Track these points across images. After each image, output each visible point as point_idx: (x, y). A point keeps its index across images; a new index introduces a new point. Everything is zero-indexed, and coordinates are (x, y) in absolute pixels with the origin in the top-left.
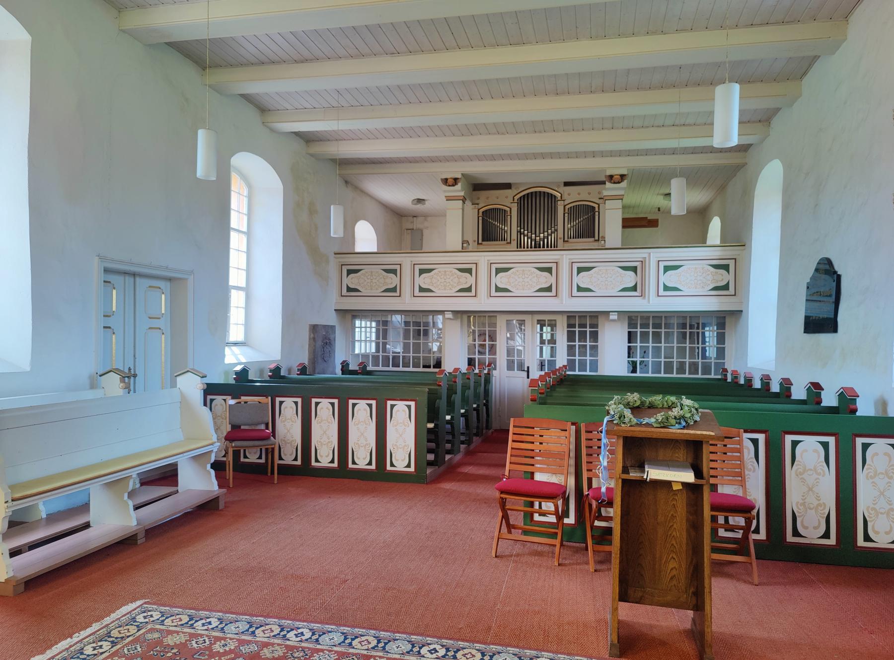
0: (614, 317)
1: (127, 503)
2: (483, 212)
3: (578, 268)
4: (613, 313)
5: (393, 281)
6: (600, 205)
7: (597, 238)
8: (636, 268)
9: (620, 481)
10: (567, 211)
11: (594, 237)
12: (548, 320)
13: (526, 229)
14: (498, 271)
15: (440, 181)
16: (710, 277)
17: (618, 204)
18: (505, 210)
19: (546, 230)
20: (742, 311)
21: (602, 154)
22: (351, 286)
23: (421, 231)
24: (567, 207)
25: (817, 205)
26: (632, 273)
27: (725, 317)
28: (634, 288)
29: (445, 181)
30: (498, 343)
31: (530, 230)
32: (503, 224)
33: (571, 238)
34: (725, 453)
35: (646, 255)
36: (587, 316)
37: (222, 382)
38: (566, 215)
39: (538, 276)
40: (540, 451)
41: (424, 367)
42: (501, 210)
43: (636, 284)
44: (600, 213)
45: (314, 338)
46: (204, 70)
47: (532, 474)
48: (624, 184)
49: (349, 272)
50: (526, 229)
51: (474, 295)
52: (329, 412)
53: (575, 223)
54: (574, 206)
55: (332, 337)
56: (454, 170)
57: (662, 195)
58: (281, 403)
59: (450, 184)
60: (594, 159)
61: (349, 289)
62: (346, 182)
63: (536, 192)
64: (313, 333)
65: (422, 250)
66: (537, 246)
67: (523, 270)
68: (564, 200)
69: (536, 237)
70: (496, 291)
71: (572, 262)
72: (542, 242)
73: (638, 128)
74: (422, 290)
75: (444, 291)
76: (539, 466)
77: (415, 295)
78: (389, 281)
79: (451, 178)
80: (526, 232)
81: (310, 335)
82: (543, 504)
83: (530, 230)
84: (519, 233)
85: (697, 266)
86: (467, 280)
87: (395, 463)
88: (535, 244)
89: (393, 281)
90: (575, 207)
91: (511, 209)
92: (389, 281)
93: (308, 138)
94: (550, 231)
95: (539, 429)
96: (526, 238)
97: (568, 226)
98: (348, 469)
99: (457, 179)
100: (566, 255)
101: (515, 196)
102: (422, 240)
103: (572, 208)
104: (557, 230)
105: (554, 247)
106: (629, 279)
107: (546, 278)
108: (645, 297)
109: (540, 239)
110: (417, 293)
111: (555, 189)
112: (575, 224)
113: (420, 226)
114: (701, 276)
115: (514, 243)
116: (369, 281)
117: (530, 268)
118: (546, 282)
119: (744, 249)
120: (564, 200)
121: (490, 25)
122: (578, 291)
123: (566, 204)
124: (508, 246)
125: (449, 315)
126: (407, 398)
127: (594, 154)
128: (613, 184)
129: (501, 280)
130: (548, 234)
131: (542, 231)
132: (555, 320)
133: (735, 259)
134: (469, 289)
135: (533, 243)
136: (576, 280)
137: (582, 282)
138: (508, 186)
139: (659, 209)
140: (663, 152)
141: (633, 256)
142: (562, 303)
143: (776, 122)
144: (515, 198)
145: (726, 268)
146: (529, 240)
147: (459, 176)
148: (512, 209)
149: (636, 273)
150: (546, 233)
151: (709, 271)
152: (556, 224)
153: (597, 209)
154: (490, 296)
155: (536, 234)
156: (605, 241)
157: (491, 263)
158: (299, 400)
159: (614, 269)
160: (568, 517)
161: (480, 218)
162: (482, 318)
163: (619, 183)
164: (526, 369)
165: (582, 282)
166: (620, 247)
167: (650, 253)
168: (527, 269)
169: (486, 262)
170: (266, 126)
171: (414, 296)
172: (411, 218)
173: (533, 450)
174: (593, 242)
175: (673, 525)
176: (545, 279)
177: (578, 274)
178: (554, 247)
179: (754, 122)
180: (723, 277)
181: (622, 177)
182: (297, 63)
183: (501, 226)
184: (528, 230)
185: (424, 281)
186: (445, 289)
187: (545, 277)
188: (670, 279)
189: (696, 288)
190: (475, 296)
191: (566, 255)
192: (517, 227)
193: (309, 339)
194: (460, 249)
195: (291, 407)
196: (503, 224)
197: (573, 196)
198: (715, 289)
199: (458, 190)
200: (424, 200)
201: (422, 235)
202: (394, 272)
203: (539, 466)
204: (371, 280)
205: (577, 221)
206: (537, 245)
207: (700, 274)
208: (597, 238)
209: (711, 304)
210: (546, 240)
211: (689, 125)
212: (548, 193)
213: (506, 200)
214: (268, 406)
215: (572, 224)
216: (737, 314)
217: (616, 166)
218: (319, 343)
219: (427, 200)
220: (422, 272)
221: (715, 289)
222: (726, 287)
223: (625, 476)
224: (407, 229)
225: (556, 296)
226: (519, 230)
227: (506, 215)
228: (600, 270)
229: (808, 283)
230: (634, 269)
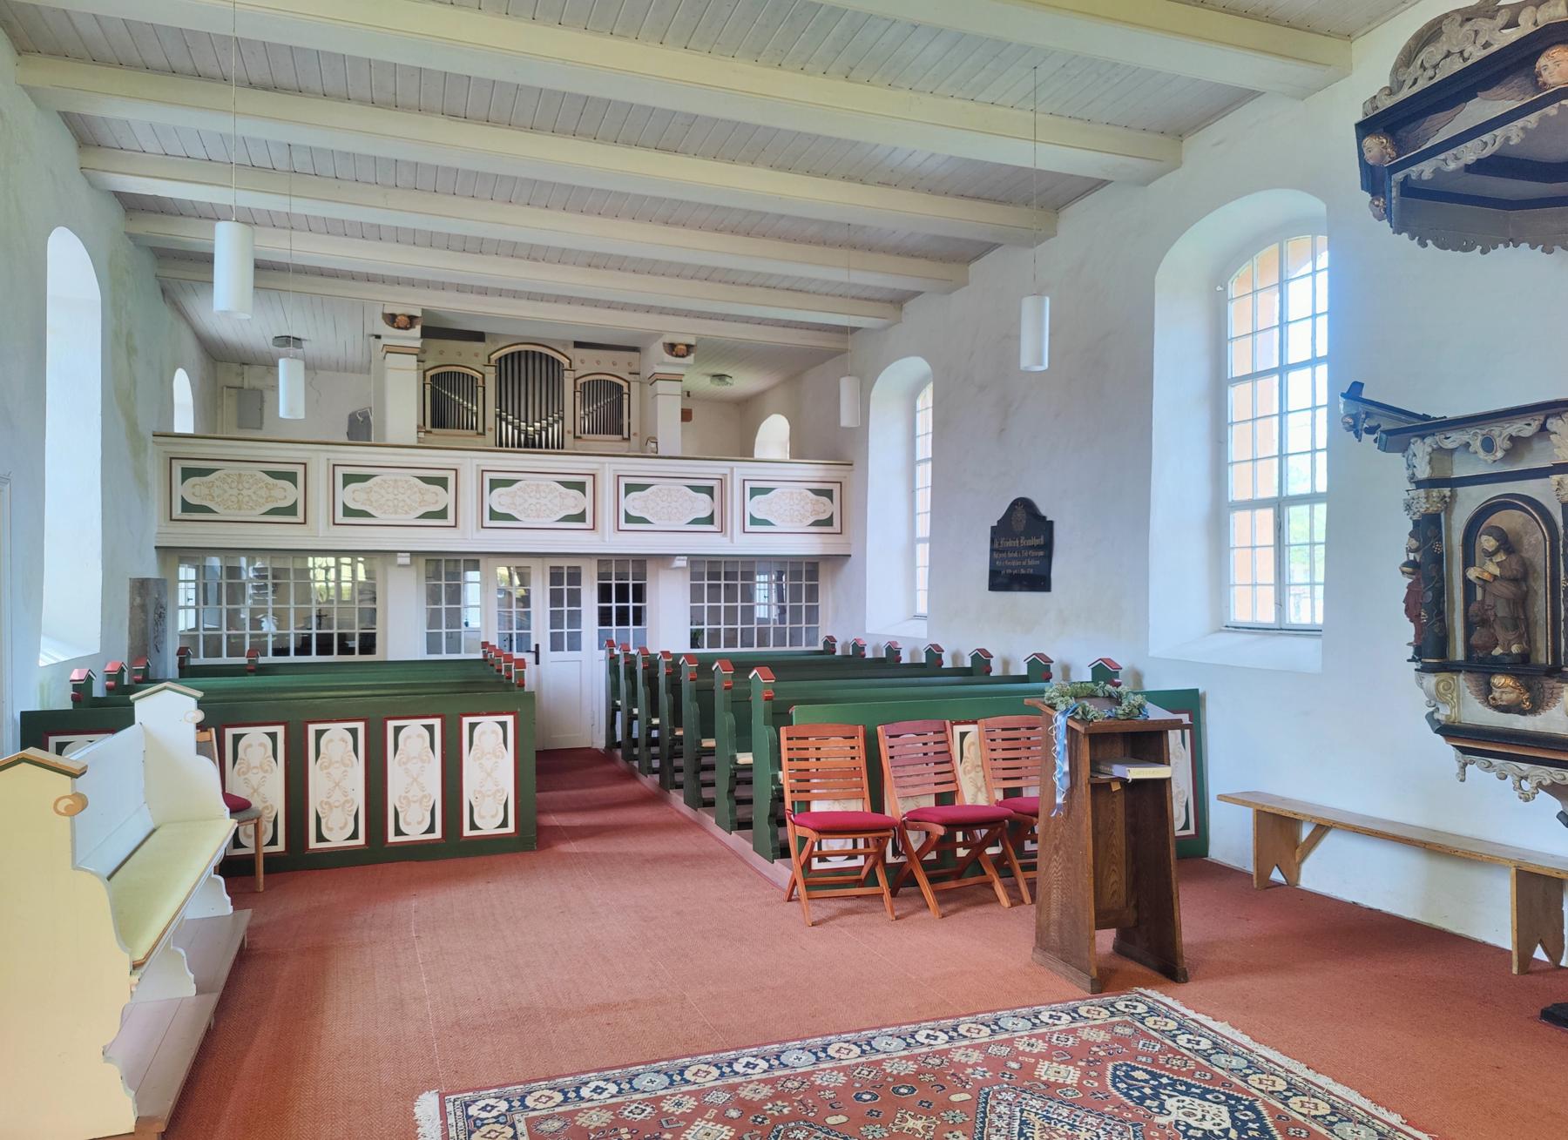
0: (681, 563)
1: (178, 952)
2: (432, 377)
3: (626, 485)
4: (682, 558)
5: (286, 494)
6: (632, 383)
7: (626, 435)
8: (712, 488)
9: (1089, 786)
10: (578, 387)
11: (621, 433)
12: (568, 567)
13: (510, 411)
14: (494, 484)
15: (381, 316)
16: (809, 507)
17: (676, 388)
18: (472, 377)
19: (544, 416)
20: (850, 556)
21: (662, 311)
22: (192, 500)
23: (261, 391)
24: (579, 382)
25: (1003, 430)
26: (706, 497)
27: (817, 563)
28: (710, 520)
29: (391, 319)
30: (533, 609)
31: (516, 415)
32: (470, 398)
33: (584, 432)
34: (1029, 748)
35: (727, 471)
36: (611, 561)
37: (38, 709)
38: (578, 394)
39: (563, 496)
40: (855, 768)
41: (277, 652)
42: (465, 376)
43: (713, 513)
44: (631, 396)
45: (143, 607)
46: (19, 54)
47: (808, 803)
48: (690, 359)
49: (187, 473)
50: (510, 411)
51: (453, 524)
52: (346, 746)
53: (591, 408)
54: (589, 382)
55: (164, 601)
56: (411, 303)
57: (708, 375)
58: (237, 739)
59: (401, 326)
60: (647, 314)
61: (187, 507)
62: (163, 292)
63: (527, 352)
64: (141, 596)
65: (260, 428)
66: (529, 444)
67: (538, 485)
68: (574, 371)
69: (527, 426)
70: (491, 519)
71: (618, 476)
72: (537, 436)
73: (742, 284)
74: (348, 512)
75: (393, 516)
76: (815, 791)
77: (336, 522)
78: (277, 493)
79: (404, 315)
80: (510, 418)
81: (132, 599)
82: (824, 841)
83: (516, 415)
84: (498, 419)
86: (437, 498)
87: (478, 822)
88: (526, 437)
89: (286, 494)
90: (591, 383)
91: (483, 375)
92: (277, 493)
93: (133, 205)
94: (550, 419)
95: (814, 739)
96: (510, 427)
97: (580, 413)
98: (387, 846)
99: (416, 317)
100: (610, 463)
101: (492, 354)
102: (261, 409)
103: (587, 385)
104: (563, 419)
105: (558, 447)
106: (702, 505)
107: (576, 499)
108: (725, 535)
109: (534, 431)
110: (340, 518)
111: (557, 348)
112: (591, 410)
113: (257, 384)
114: (797, 504)
115: (490, 435)
116: (235, 492)
117: (549, 483)
118: (576, 505)
119: (852, 470)
120: (574, 371)
121: (649, 118)
122: (626, 522)
123: (577, 376)
124: (480, 439)
125: (404, 559)
126: (500, 710)
127: (649, 309)
128: (674, 358)
129: (500, 500)
130: (548, 424)
131: (537, 418)
132: (579, 567)
133: (841, 483)
134: (442, 514)
135: (523, 436)
138: (479, 337)
139: (688, 395)
140: (747, 320)
141: (709, 470)
142: (604, 541)
143: (910, 306)
144: (492, 357)
145: (828, 494)
146: (516, 432)
147: (419, 314)
148: (487, 376)
149: (712, 498)
150: (544, 422)
152: (561, 409)
153: (626, 390)
154: (482, 527)
155: (526, 422)
156: (657, 443)
157: (483, 471)
158: (280, 730)
159: (680, 488)
160: (819, 862)
161: (428, 387)
162: (452, 564)
163: (683, 356)
164: (533, 649)
165: (633, 507)
166: (679, 454)
167: (732, 469)
168: (544, 483)
169: (475, 468)
170: (85, 175)
171: (334, 524)
172: (235, 367)
173: (808, 770)
174: (619, 441)
175: (1112, 833)
176: (573, 502)
177: (627, 493)
178: (558, 448)
179: (885, 301)
180: (825, 508)
181: (689, 347)
182: (255, 88)
183: (465, 403)
184: (513, 415)
185: (353, 496)
186: (396, 513)
187: (573, 497)
188: (757, 506)
189: (792, 521)
190: (455, 526)
191: (610, 463)
192: (496, 408)
193: (131, 608)
194: (414, 442)
195: (261, 745)
196: (470, 398)
197: (587, 365)
198: (816, 523)
199: (413, 336)
200: (299, 339)
201: (262, 401)
202: (291, 477)
203: (815, 791)
204: (239, 490)
205: (595, 406)
206: (530, 442)
207: (797, 502)
208: (626, 435)
209: (809, 545)
210: (544, 433)
211: (808, 292)
212: (547, 355)
213: (475, 360)
214: (212, 746)
215: (587, 410)
216: (837, 560)
217: (683, 332)
218: (152, 616)
219: (305, 340)
220: (349, 479)
221: (816, 523)
222: (828, 522)
223: (1094, 781)
224: (228, 387)
225: (593, 529)
226: (498, 413)
227: (475, 385)
229: (992, 527)
230: (709, 491)
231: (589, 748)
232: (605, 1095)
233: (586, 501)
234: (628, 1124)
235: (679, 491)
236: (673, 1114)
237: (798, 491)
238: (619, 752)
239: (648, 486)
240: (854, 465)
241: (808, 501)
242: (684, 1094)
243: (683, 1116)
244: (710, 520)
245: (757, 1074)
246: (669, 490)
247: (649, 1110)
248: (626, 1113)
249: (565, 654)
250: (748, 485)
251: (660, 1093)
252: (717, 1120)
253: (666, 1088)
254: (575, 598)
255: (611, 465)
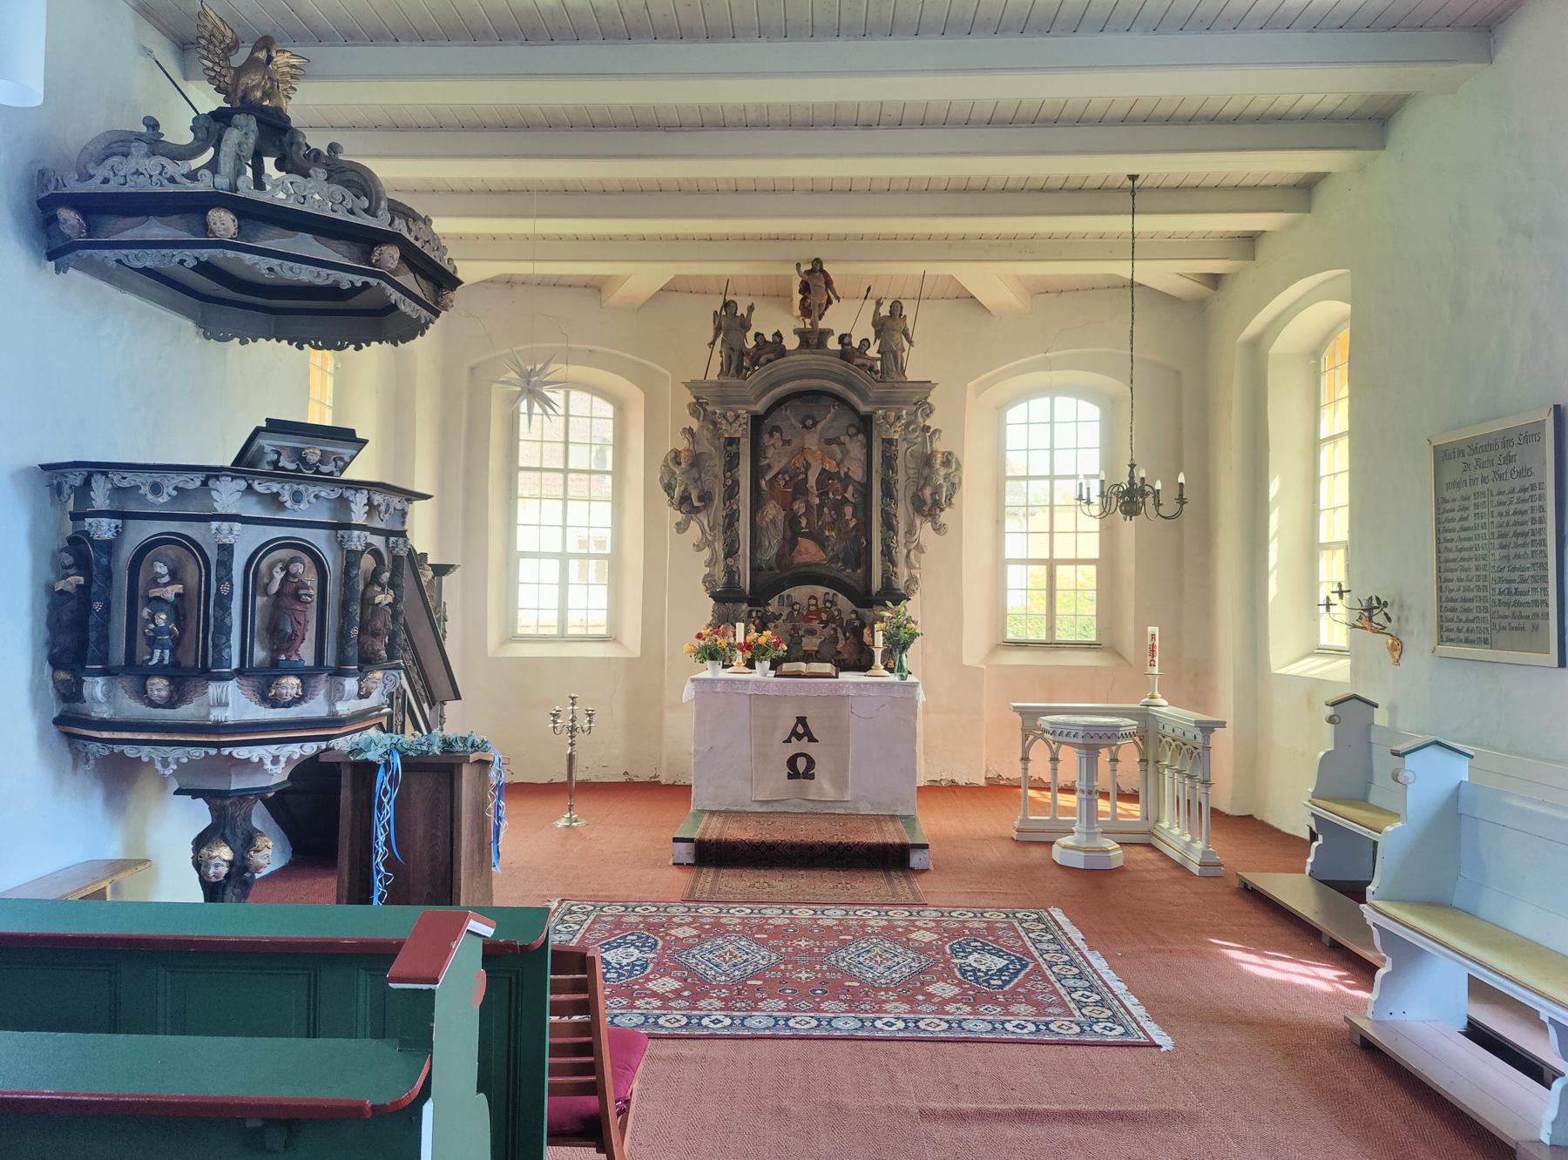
232: (1015, 1023)
234: (999, 1004)
236: (965, 1003)
242: (952, 1014)
243: (957, 1001)
245: (888, 1018)
247: (981, 1009)
248: (999, 1010)
251: (972, 1017)
252: (934, 996)
253: (965, 1020)
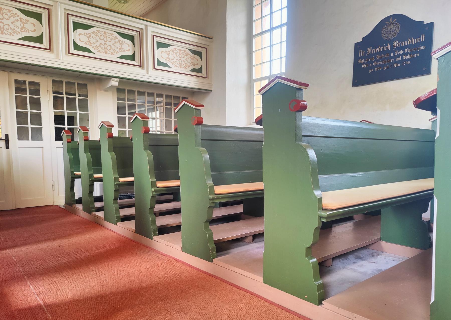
4: (116, 79)
16: (189, 60)
20: (212, 91)
28: (133, 57)
35: (143, 27)
85: (181, 49)
107: (34, 26)
118: (35, 30)
122: (75, 49)
136: (72, 35)
137: (80, 39)
145: (199, 54)
151: (189, 55)
165: (80, 39)
168: (6, 8)
177: (74, 30)
188: (161, 54)
189: (181, 67)
198: (194, 70)
207: (183, 56)
221: (194, 70)
222: (199, 70)
228: (99, 31)
230: (132, 38)
231: (52, 205)
233: (44, 30)
235: (112, 35)
237: (183, 49)
238: (80, 207)
239: (91, 27)
240: (214, 39)
241: (189, 56)
244: (133, 57)
246: (105, 32)
249: (30, 143)
250: (156, 39)
254: (36, 103)
255: (62, 5)
